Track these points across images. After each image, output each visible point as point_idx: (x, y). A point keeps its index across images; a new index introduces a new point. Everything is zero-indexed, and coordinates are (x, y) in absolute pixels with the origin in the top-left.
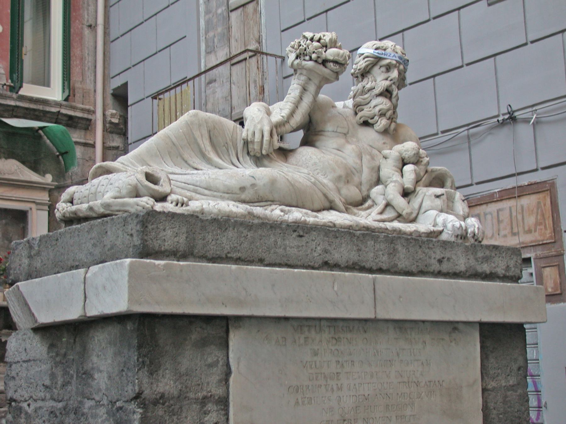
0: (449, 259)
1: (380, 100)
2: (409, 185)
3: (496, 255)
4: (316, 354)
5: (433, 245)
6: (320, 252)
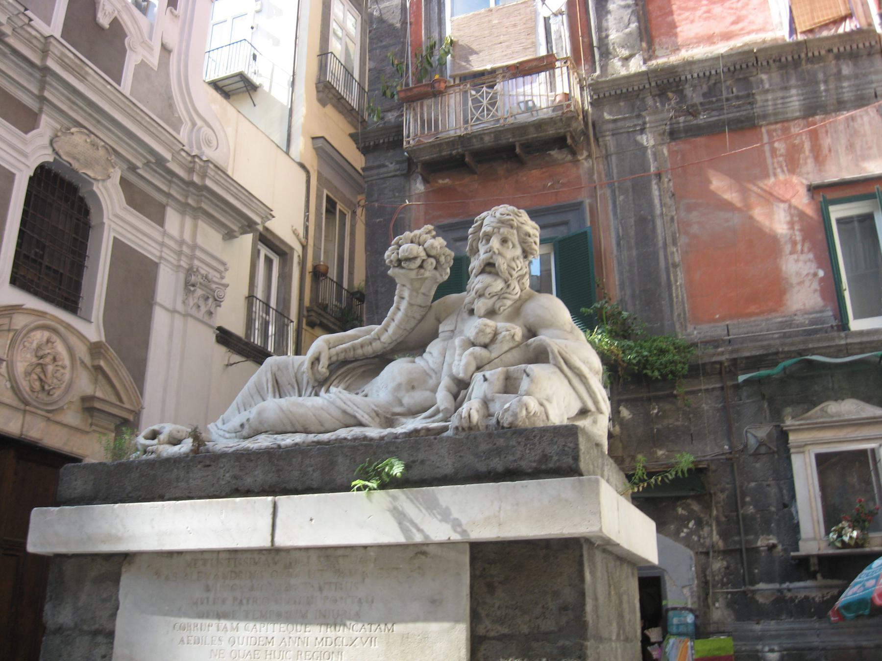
0: (423, 462)
1: (480, 277)
2: (461, 375)
3: (519, 443)
4: (208, 589)
5: (397, 448)
6: (229, 479)
